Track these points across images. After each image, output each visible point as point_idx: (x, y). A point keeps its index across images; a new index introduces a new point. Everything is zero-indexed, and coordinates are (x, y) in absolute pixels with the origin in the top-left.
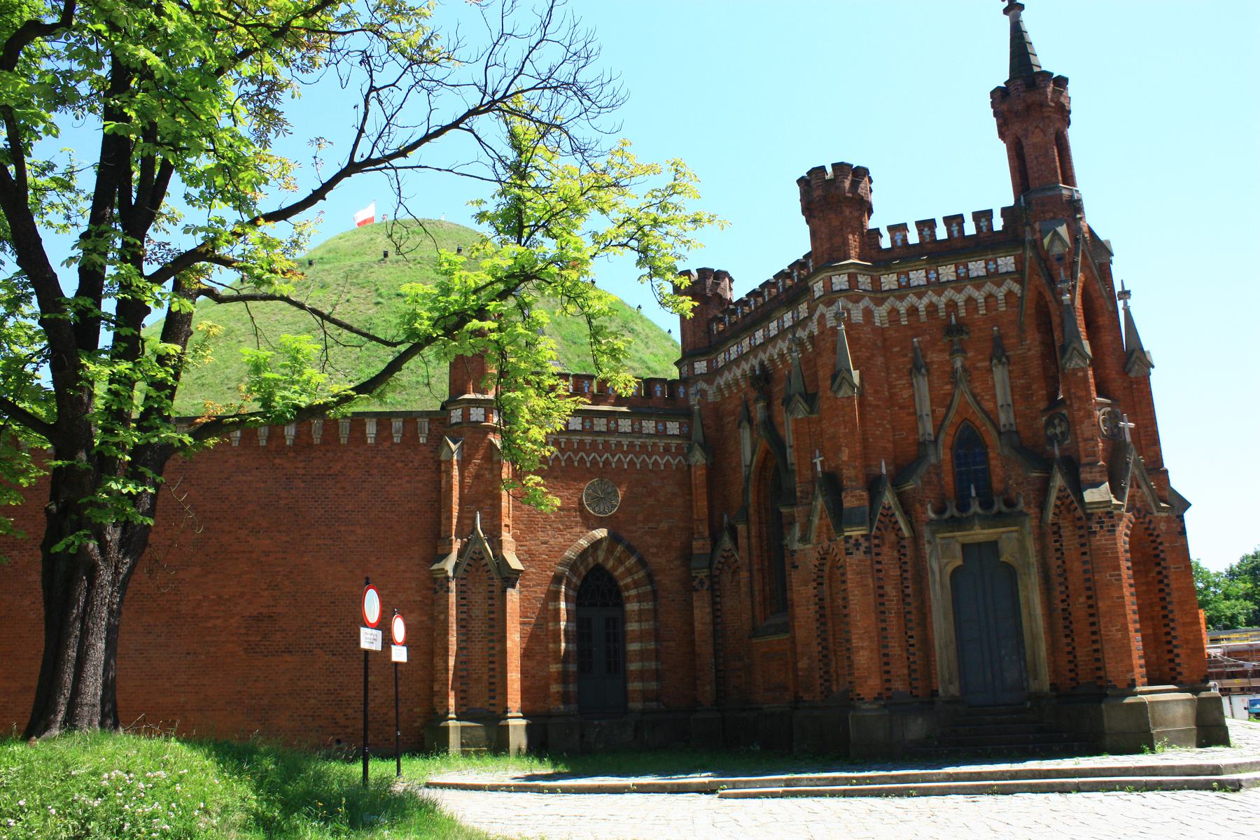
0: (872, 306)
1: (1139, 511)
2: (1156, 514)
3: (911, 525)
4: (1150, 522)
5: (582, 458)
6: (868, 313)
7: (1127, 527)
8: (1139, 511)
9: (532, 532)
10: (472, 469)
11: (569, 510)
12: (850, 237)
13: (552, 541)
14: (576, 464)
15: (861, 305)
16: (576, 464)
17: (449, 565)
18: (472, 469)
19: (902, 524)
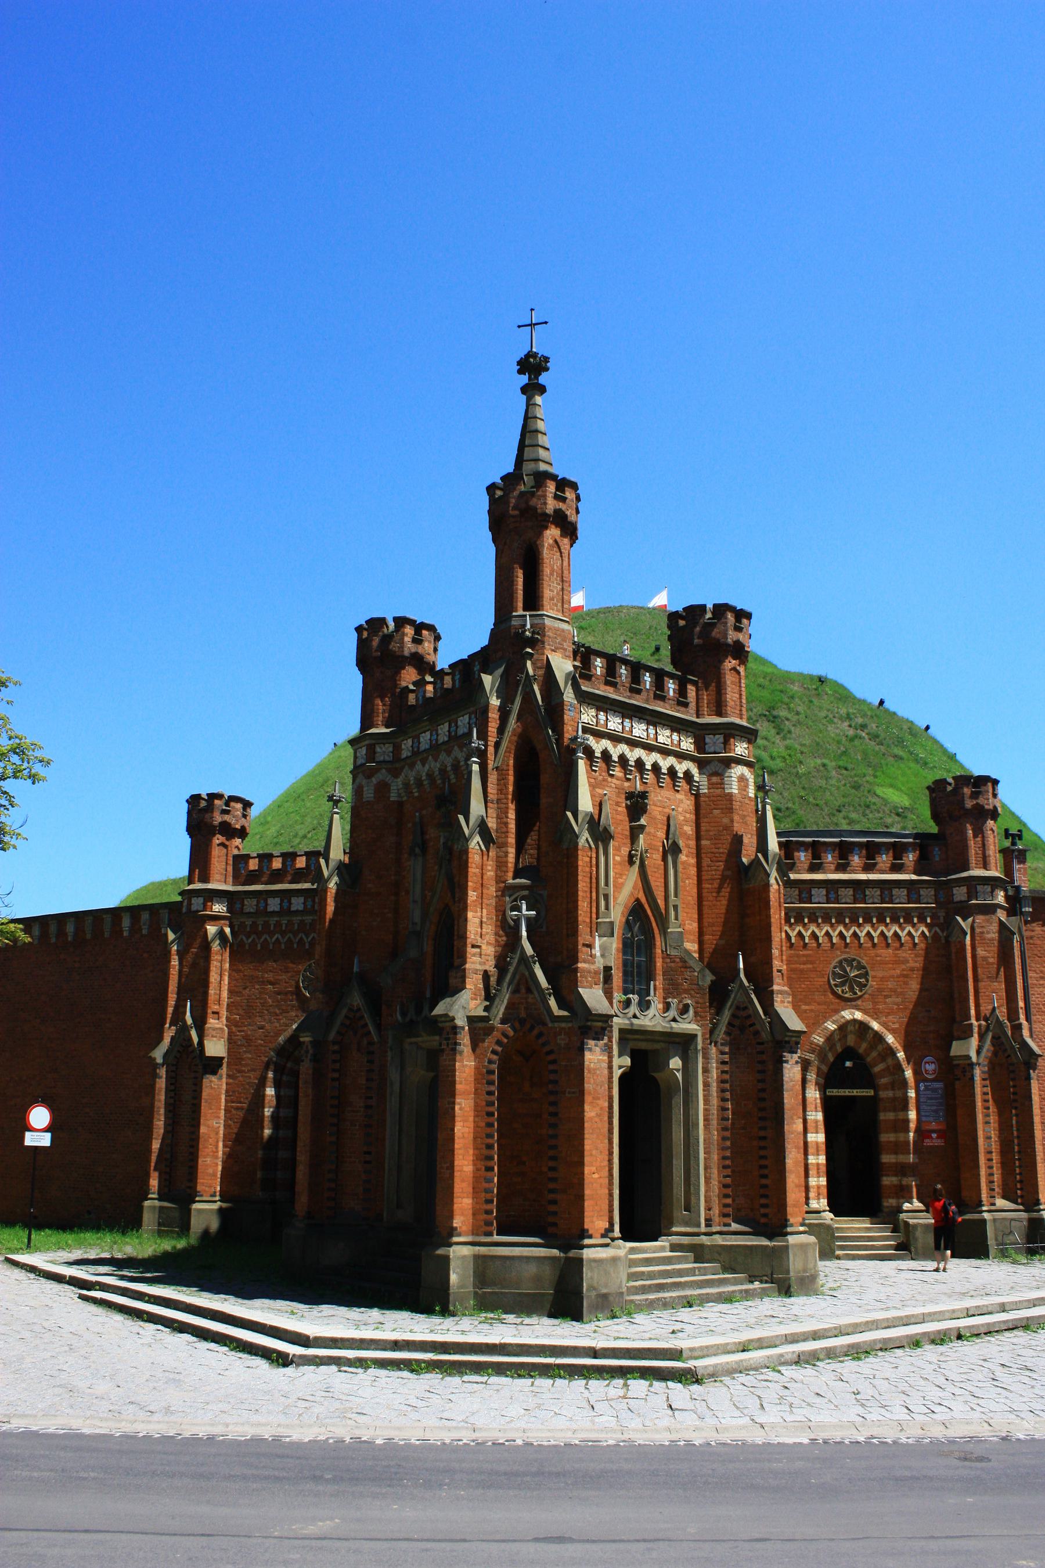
0: (389, 778)
1: (522, 1022)
2: (550, 1025)
3: (379, 1027)
4: (540, 1035)
5: (301, 939)
6: (382, 788)
7: (499, 1043)
8: (522, 1022)
9: (250, 1017)
10: (189, 958)
11: (286, 994)
12: (378, 702)
13: (268, 1026)
14: (295, 946)
15: (374, 780)
16: (295, 946)
17: (158, 1054)
18: (189, 958)
19: (371, 1028)
